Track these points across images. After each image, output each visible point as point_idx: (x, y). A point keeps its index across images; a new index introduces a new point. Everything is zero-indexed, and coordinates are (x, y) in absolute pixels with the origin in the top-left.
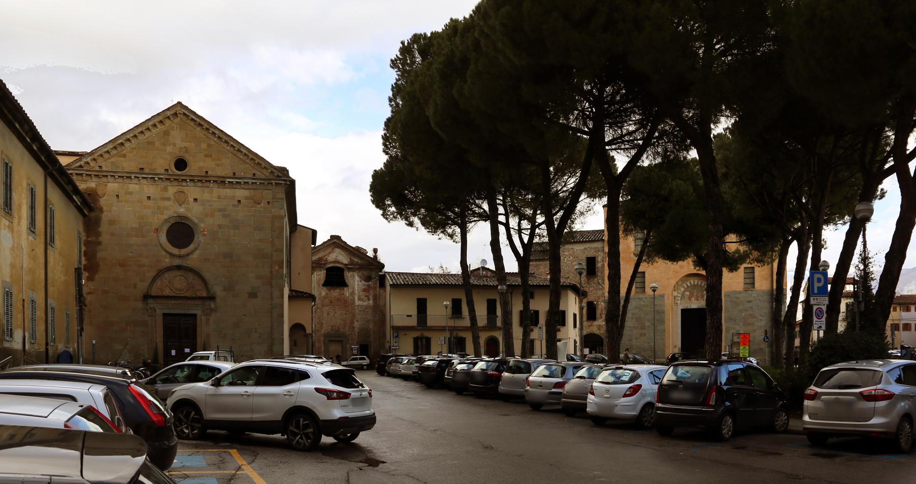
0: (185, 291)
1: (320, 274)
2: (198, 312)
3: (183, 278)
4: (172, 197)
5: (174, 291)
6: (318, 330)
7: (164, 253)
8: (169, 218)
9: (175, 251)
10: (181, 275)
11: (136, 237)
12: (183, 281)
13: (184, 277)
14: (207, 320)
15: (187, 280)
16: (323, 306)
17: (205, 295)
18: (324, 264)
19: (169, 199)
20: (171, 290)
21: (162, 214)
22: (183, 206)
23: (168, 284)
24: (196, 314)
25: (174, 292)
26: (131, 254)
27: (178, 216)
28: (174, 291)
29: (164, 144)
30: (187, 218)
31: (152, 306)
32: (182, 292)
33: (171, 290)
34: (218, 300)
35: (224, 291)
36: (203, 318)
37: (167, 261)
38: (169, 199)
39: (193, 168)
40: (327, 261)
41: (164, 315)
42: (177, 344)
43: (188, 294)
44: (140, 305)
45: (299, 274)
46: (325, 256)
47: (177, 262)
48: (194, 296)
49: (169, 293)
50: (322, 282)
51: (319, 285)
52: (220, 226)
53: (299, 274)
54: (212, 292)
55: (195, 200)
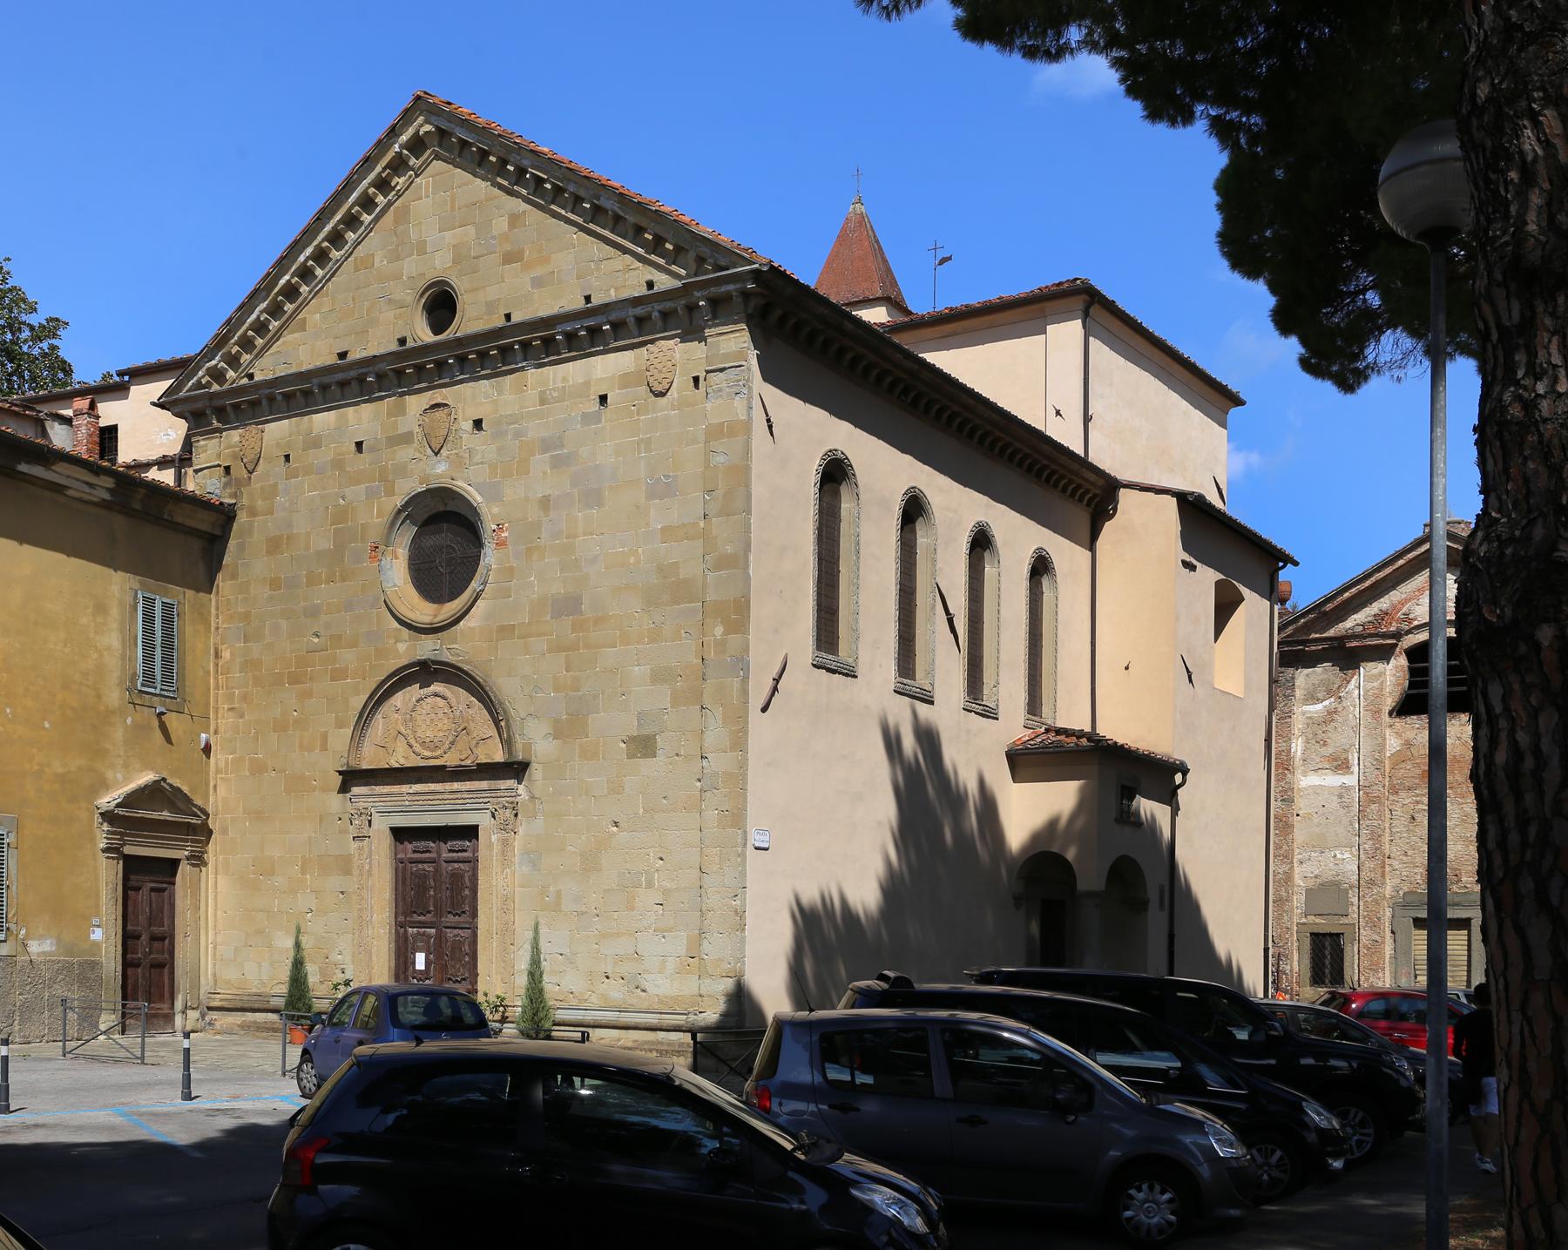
1: (1381, 674)
2: (482, 819)
4: (417, 429)
5: (417, 748)
6: (1372, 882)
7: (396, 624)
9: (423, 611)
13: (444, 698)
14: (505, 843)
16: (1394, 791)
17: (499, 756)
18: (1398, 635)
19: (407, 438)
20: (411, 746)
21: (390, 493)
22: (444, 452)
23: (403, 730)
24: (478, 826)
25: (418, 755)
26: (316, 640)
28: (417, 748)
29: (395, 257)
31: (361, 805)
32: (438, 753)
33: (411, 746)
34: (536, 771)
36: (494, 838)
37: (408, 650)
38: (407, 438)
39: (471, 320)
40: (1410, 621)
41: (400, 834)
42: (433, 931)
43: (451, 760)
44: (335, 802)
45: (1127, 668)
46: (1407, 601)
47: (427, 648)
48: (468, 762)
49: (406, 758)
50: (1390, 702)
51: (1377, 713)
52: (545, 503)
53: (1127, 668)
54: (519, 743)
55: (478, 424)
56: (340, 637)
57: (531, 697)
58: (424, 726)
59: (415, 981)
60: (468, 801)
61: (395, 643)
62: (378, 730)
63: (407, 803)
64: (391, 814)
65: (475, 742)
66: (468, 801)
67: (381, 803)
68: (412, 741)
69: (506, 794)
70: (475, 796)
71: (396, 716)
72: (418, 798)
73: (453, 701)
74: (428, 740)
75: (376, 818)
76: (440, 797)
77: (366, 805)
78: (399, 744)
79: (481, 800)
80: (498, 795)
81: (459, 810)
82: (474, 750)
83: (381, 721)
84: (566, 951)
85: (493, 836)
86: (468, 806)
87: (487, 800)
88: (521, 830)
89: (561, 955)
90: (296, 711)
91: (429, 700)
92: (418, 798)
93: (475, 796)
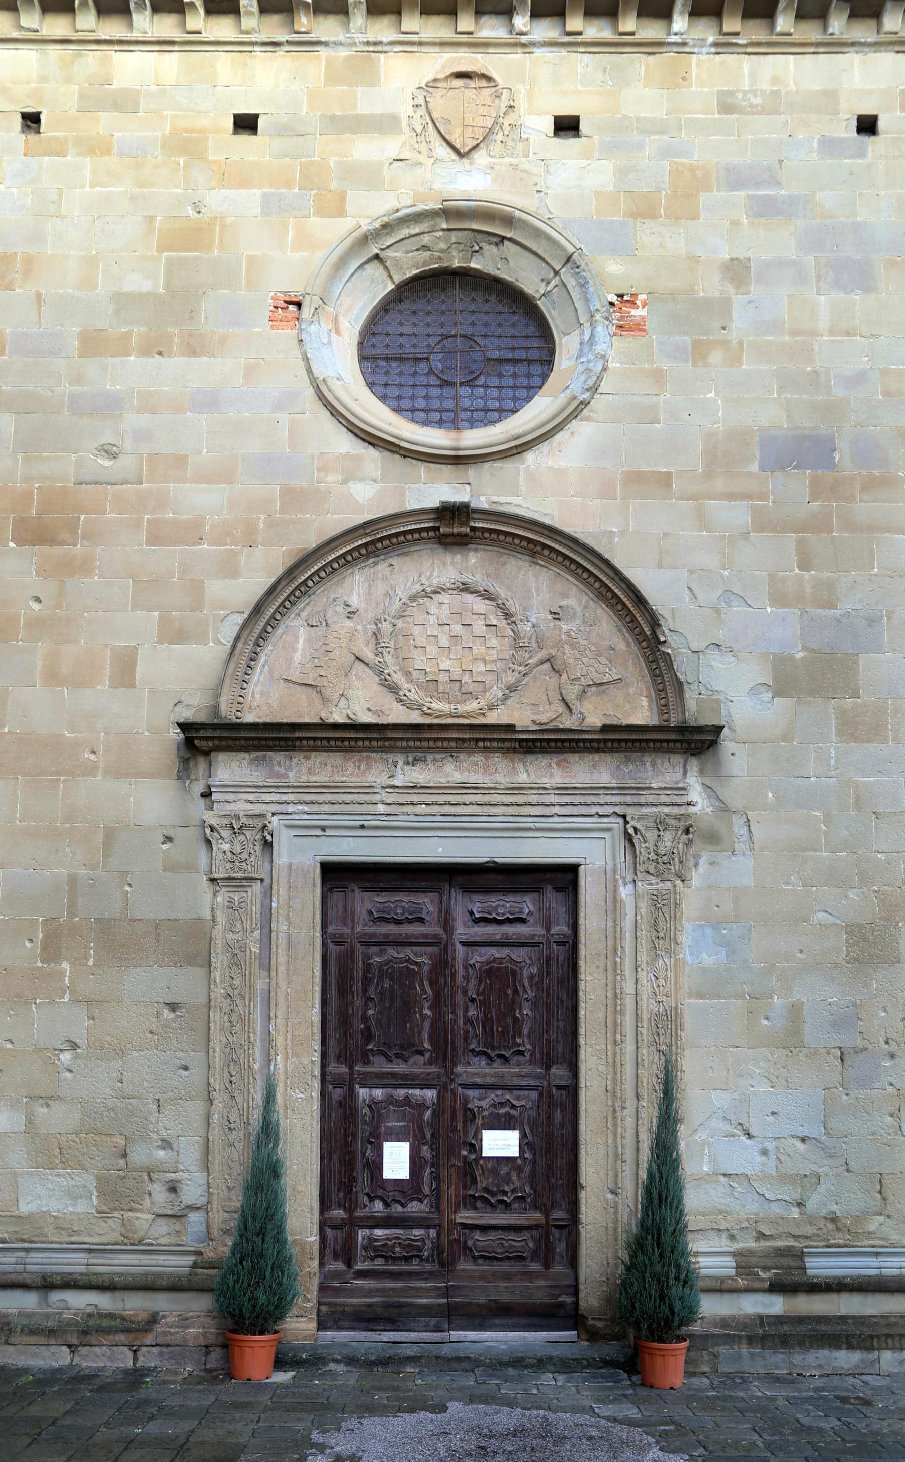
0: (496, 692)
3: (480, 605)
7: (346, 444)
8: (387, 228)
10: (465, 588)
11: (145, 352)
12: (479, 627)
13: (487, 595)
15: (507, 615)
20: (393, 689)
23: (368, 654)
27: (447, 213)
30: (508, 220)
31: (241, 806)
35: (779, 692)
36: (625, 892)
56: (180, 461)
57: (717, 611)
58: (432, 650)
59: (378, 1205)
60: (557, 810)
61: (345, 481)
62: (295, 650)
63: (381, 808)
64: (328, 832)
65: (576, 689)
66: (557, 810)
67: (300, 807)
68: (398, 678)
69: (664, 799)
70: (577, 800)
71: (349, 624)
72: (415, 799)
73: (514, 606)
74: (443, 678)
75: (284, 840)
76: (478, 799)
77: (258, 809)
78: (357, 683)
79: (593, 810)
80: (642, 800)
81: (530, 829)
82: (576, 706)
83: (303, 633)
84: (815, 1130)
85: (622, 889)
86: (555, 822)
87: (609, 810)
88: (697, 878)
89: (803, 1140)
90: (38, 600)
91: (444, 598)
92: (415, 799)
93: (577, 800)
